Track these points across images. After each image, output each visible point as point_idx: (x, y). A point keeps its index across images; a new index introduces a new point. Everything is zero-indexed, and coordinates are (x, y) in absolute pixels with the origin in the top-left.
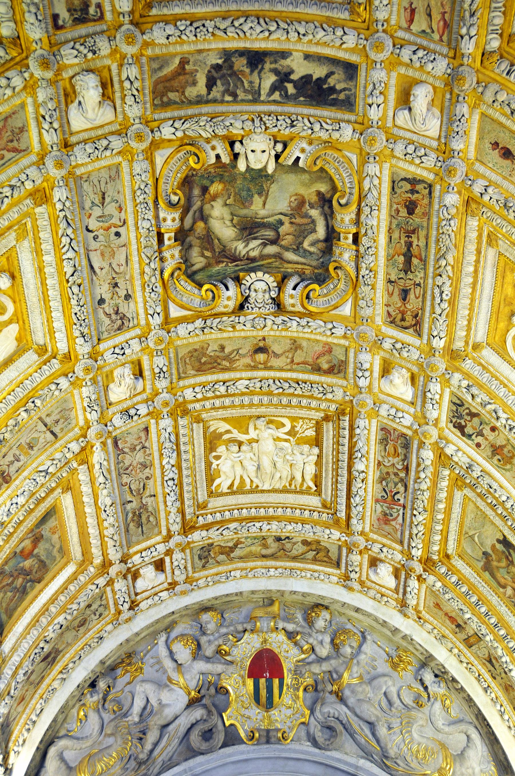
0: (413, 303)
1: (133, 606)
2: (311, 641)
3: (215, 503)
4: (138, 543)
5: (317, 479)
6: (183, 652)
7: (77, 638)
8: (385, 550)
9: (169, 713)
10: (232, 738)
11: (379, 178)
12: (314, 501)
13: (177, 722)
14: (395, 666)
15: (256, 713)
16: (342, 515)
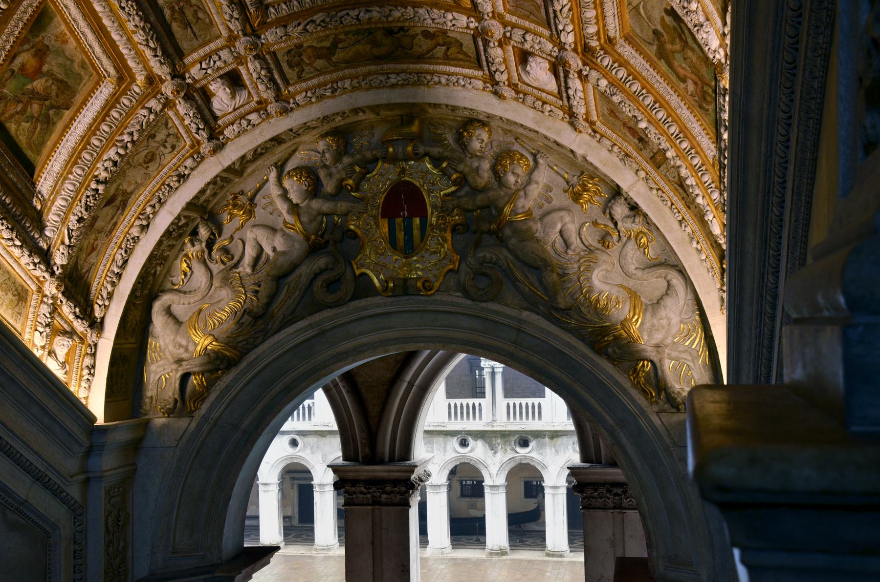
2: (461, 167)
4: (194, 50)
7: (147, 176)
8: (529, 37)
13: (297, 272)
14: (576, 197)
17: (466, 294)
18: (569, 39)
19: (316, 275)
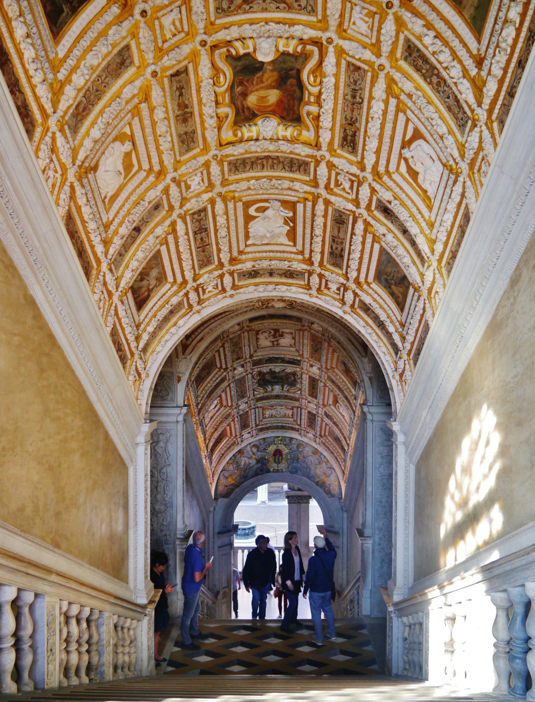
0: (314, 394)
1: (242, 441)
3: (264, 420)
5: (292, 415)
6: (255, 450)
9: (251, 465)
10: (268, 471)
11: (305, 378)
12: (292, 420)
15: (275, 465)
16: (299, 423)
17: (290, 472)
18: (318, 434)
19: (258, 468)
